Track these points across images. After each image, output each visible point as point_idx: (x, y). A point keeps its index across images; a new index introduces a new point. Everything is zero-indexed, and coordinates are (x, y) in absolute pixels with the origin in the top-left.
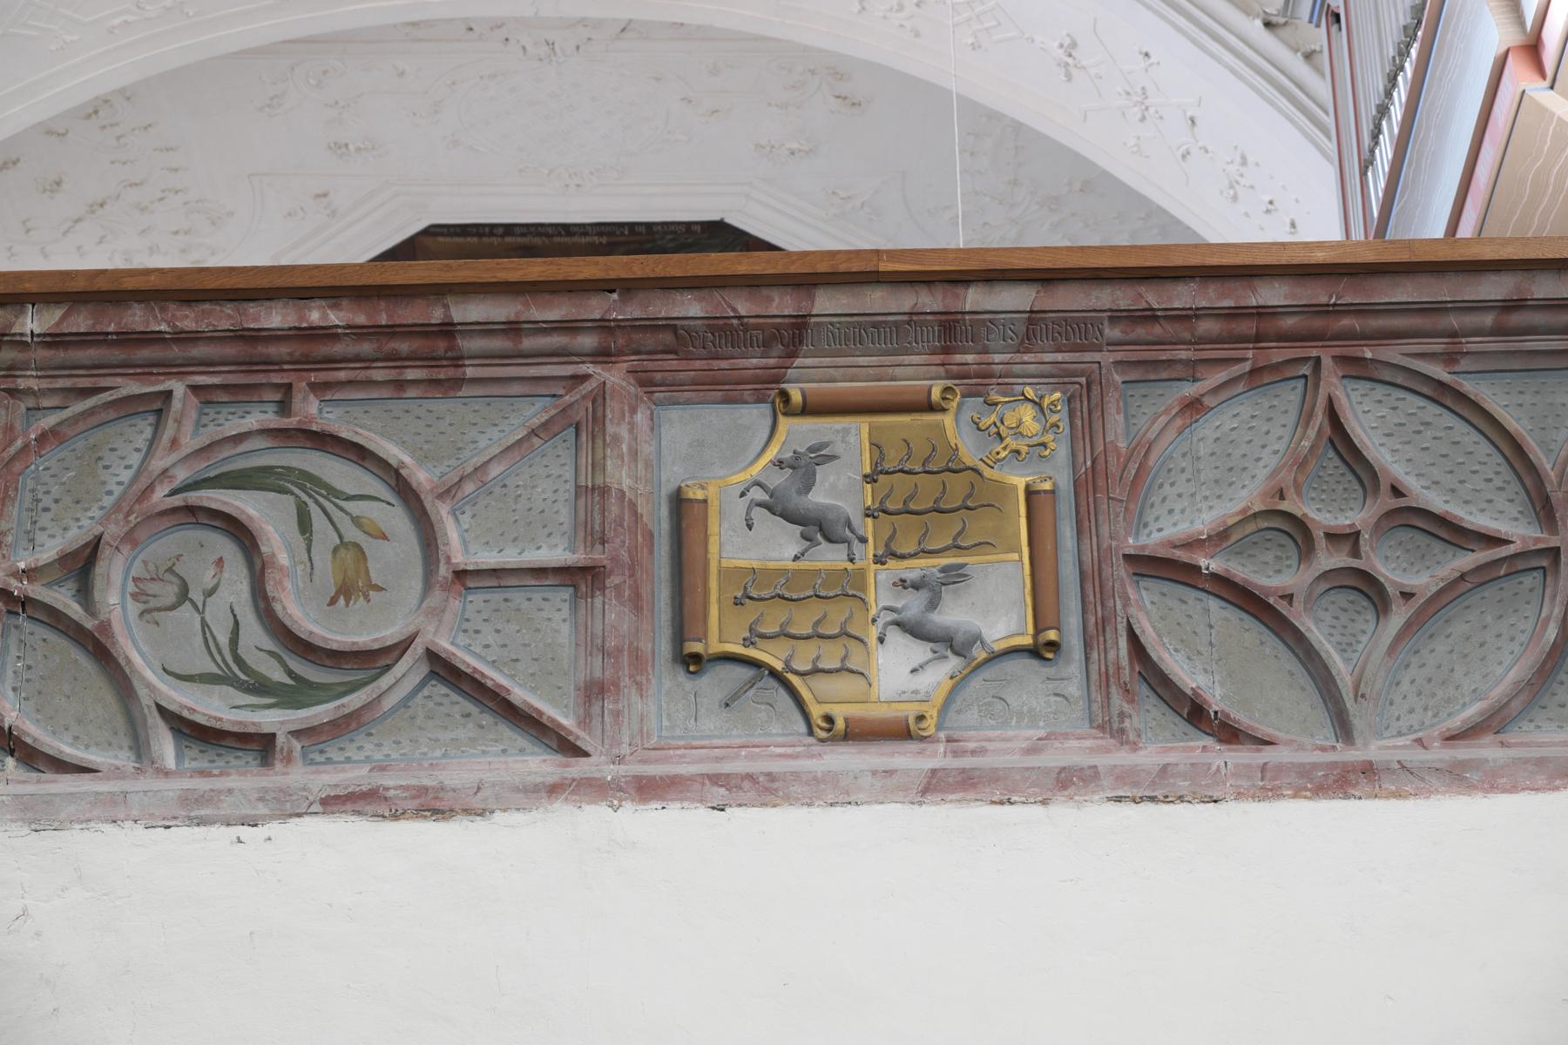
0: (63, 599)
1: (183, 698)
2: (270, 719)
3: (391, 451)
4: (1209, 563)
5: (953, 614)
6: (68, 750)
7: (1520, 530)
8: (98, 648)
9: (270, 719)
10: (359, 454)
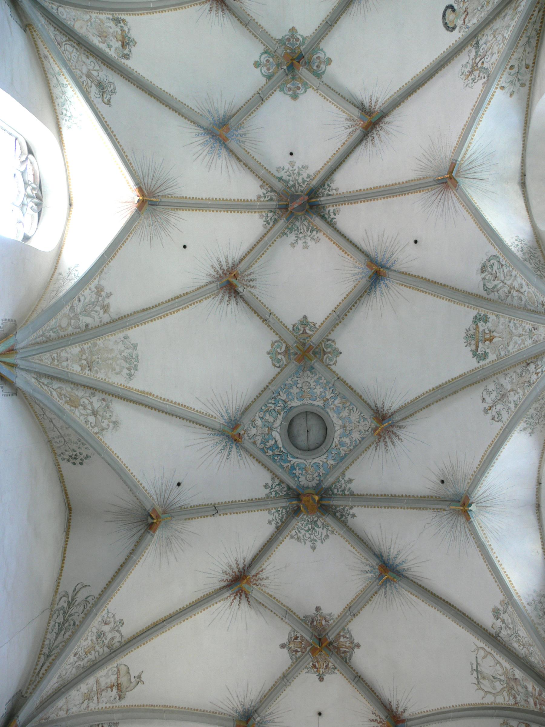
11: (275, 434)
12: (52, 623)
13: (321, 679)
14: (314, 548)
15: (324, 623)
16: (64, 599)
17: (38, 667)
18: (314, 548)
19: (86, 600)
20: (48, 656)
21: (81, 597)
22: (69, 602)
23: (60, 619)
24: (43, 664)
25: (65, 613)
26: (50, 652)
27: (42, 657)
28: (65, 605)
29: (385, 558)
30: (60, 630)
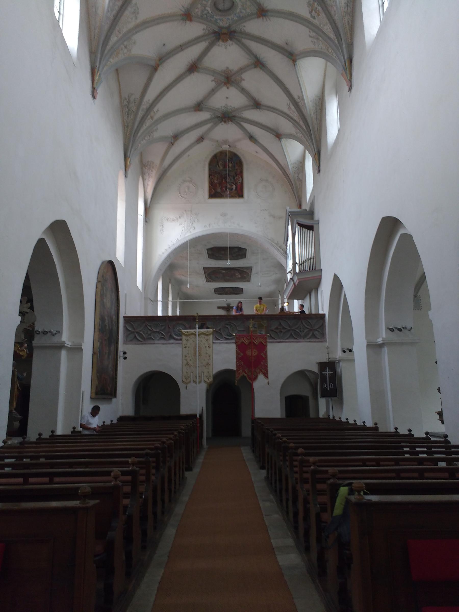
0: (219, 331)
1: (225, 337)
2: (230, 338)
3: (234, 323)
4: (274, 330)
5: (262, 333)
6: (221, 339)
7: (289, 328)
8: (221, 334)
9: (230, 338)
10: (233, 324)
11: (208, 8)
12: (124, 112)
13: (228, 88)
14: (226, 48)
15: (230, 72)
16: (125, 101)
17: (126, 132)
18: (226, 48)
19: (135, 101)
20: (128, 127)
21: (132, 99)
22: (128, 102)
23: (127, 110)
24: (127, 131)
25: (128, 107)
26: (128, 125)
27: (126, 128)
28: (127, 104)
29: (258, 57)
30: (128, 115)
